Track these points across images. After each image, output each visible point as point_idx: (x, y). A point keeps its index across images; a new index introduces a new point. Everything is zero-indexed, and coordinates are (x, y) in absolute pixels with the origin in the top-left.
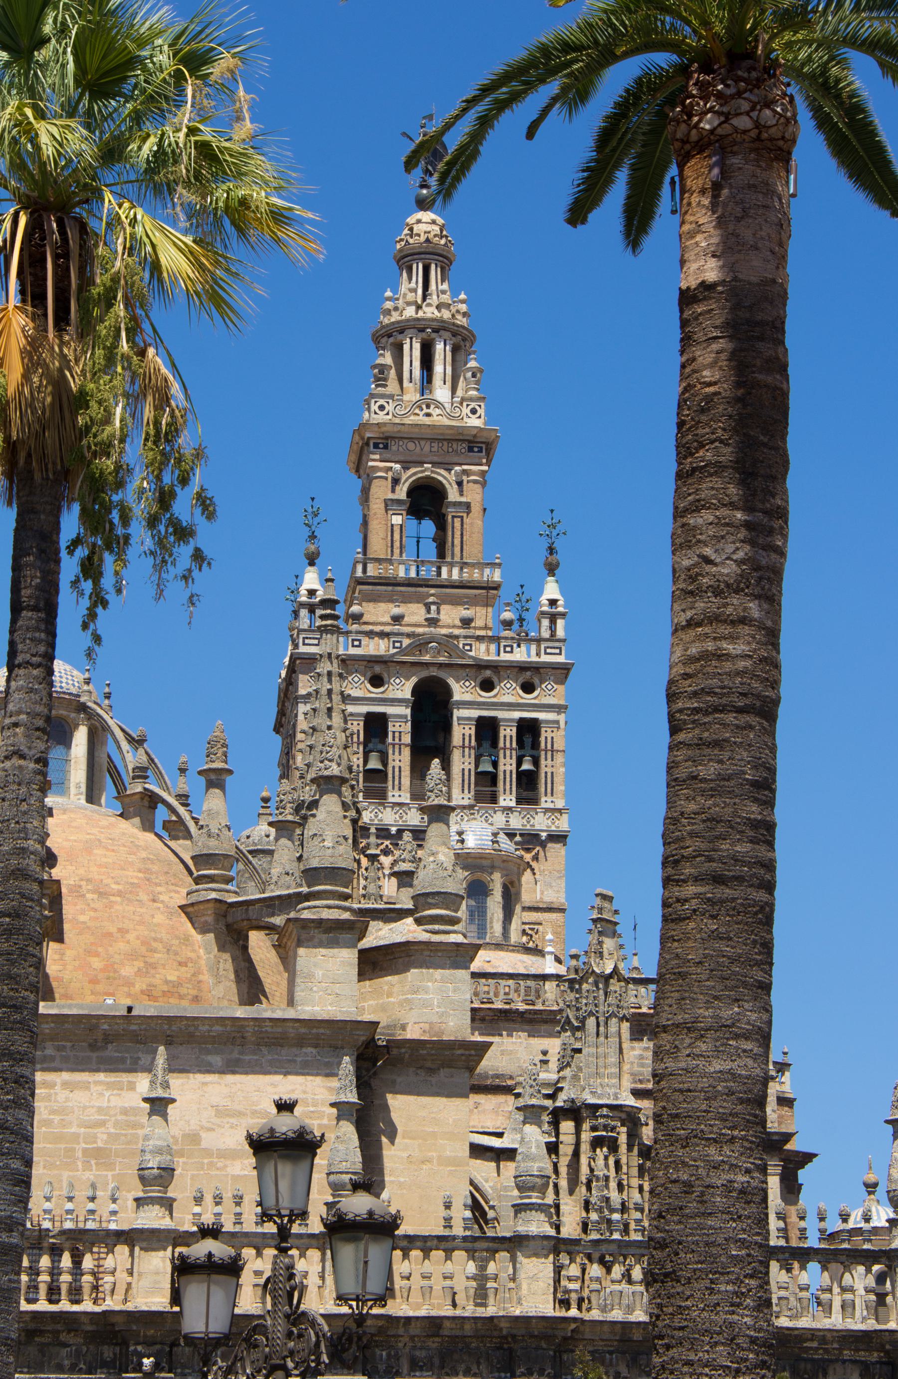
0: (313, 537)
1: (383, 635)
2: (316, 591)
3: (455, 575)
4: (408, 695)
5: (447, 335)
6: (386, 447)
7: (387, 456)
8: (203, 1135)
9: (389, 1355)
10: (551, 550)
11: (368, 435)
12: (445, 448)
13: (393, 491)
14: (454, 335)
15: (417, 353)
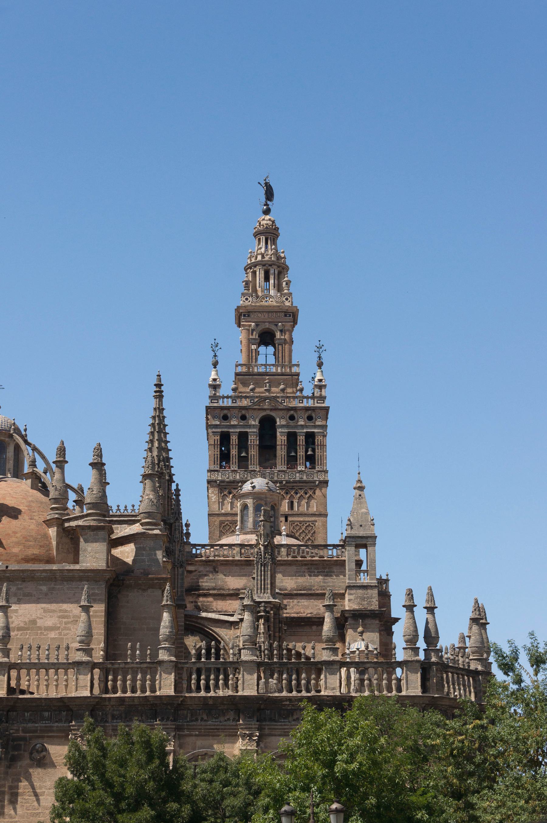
0: (215, 356)
1: (246, 397)
2: (217, 379)
3: (279, 371)
4: (257, 423)
5: (275, 267)
6: (249, 316)
7: (249, 319)
8: (38, 621)
9: (102, 714)
10: (320, 357)
11: (241, 311)
12: (274, 315)
13: (252, 335)
14: (279, 267)
15: (262, 275)
